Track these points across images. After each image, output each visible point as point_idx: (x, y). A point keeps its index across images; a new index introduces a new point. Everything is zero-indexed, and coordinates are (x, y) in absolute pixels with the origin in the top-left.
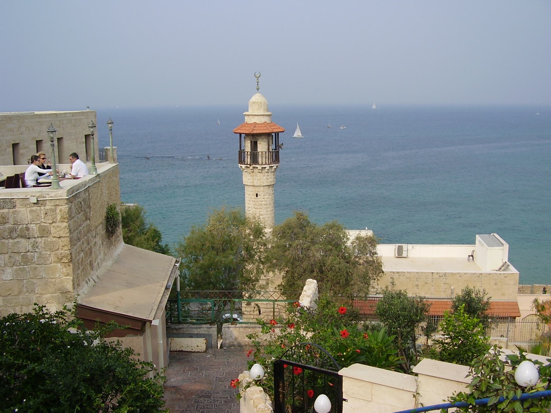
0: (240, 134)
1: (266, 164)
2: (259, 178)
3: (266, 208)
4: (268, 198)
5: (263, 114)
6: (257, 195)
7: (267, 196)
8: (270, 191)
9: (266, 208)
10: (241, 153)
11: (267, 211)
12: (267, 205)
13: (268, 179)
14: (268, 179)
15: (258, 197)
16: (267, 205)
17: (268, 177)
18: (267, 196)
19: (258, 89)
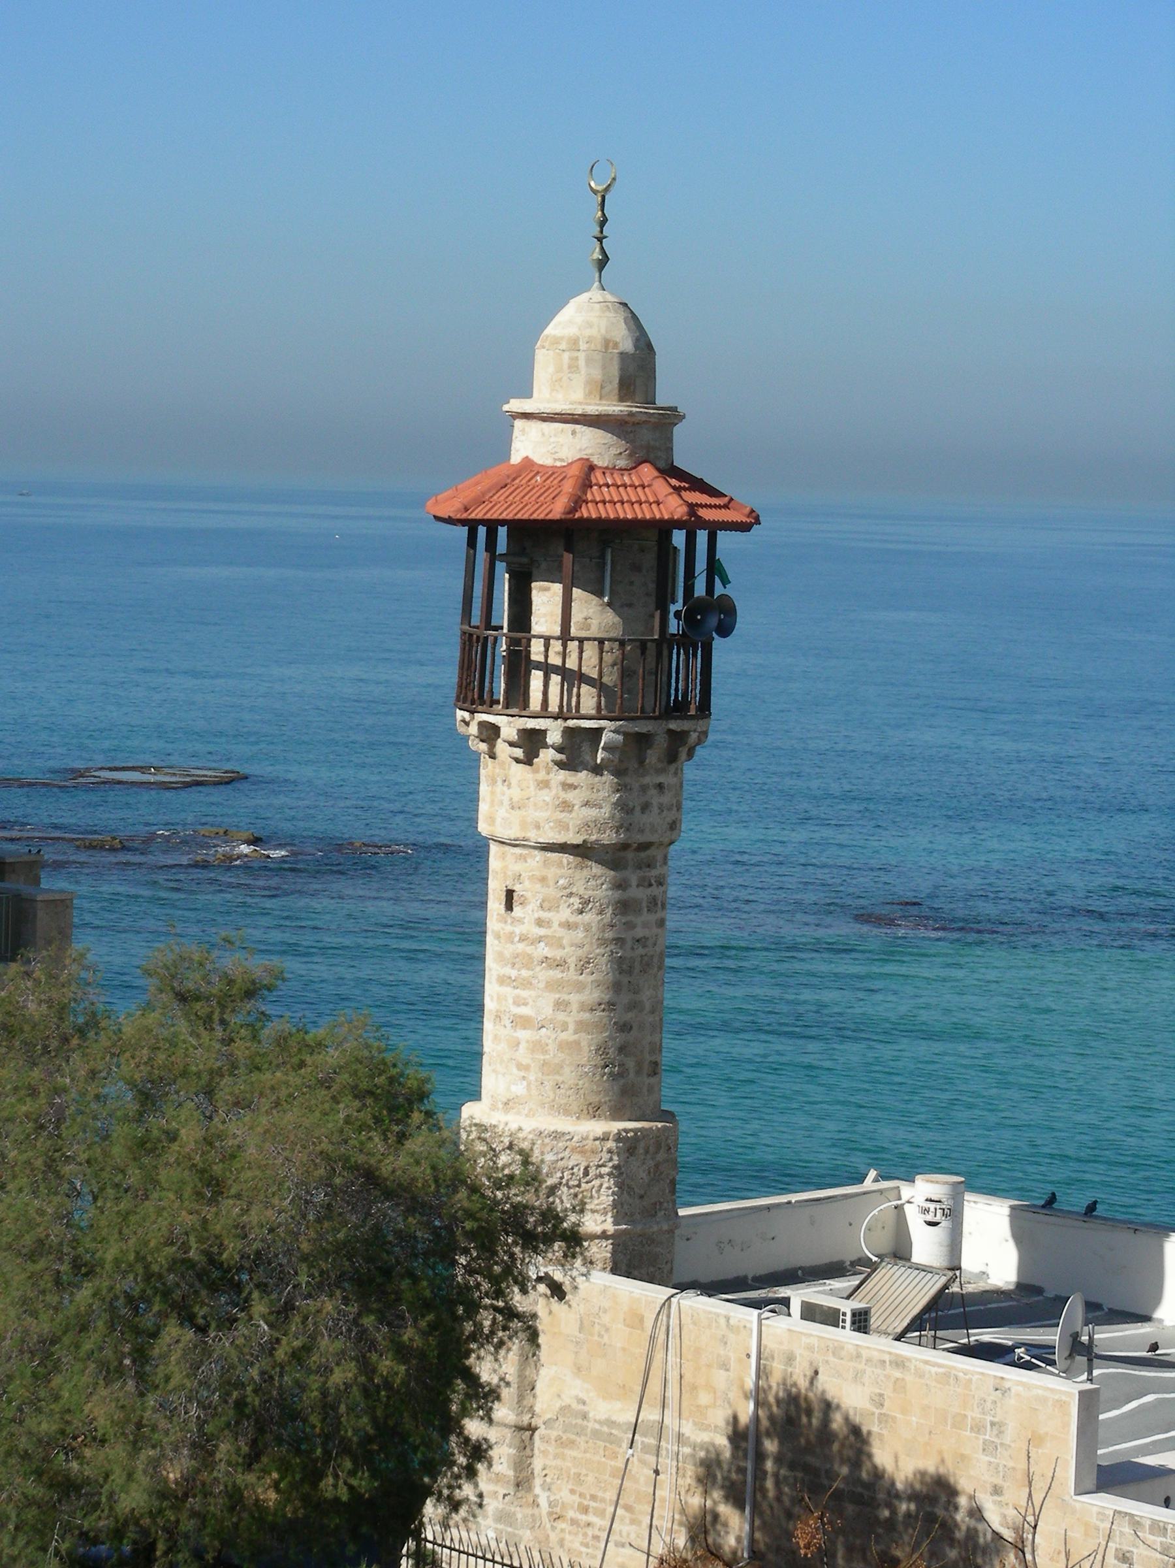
0: (472, 526)
1: (544, 713)
2: (515, 793)
3: (551, 986)
4: (568, 926)
5: (579, 411)
6: (509, 906)
7: (565, 914)
8: (593, 881)
9: (551, 986)
10: (474, 647)
11: (560, 1005)
12: (561, 964)
13: (566, 806)
14: (566, 806)
15: (518, 910)
16: (561, 964)
17: (571, 796)
18: (565, 914)
19: (602, 263)
